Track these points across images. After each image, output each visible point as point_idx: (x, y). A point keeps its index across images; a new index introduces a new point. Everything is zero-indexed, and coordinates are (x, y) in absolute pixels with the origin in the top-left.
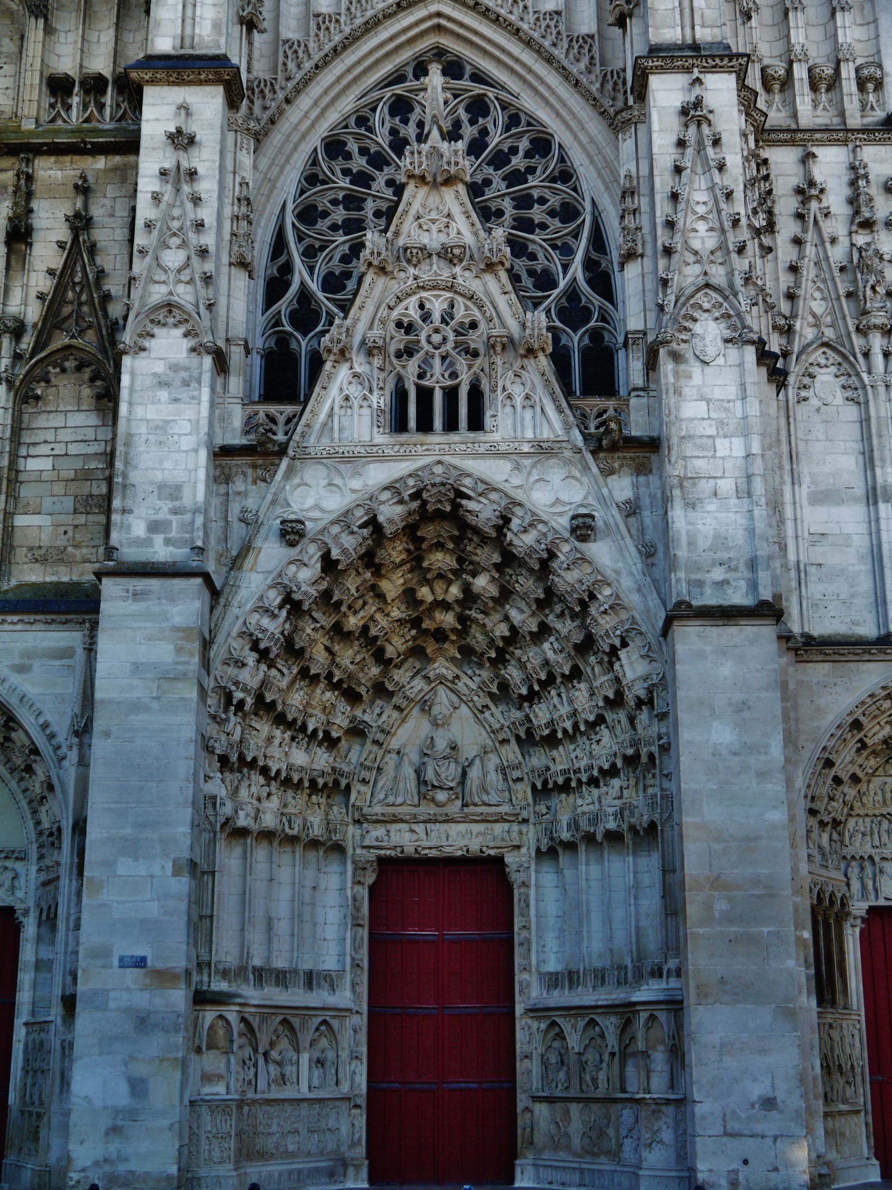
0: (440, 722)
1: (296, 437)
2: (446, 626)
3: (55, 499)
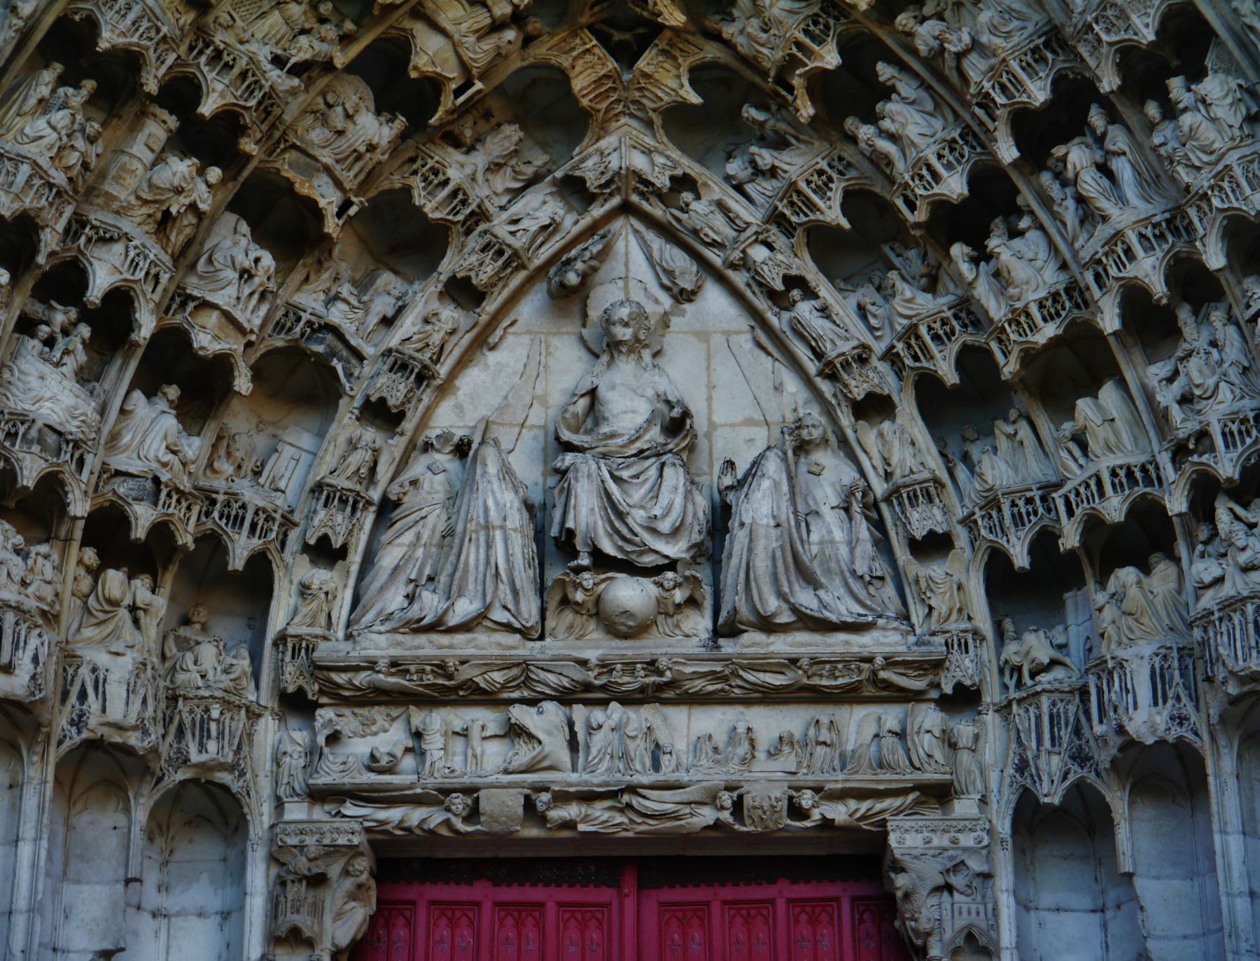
0: (624, 333)
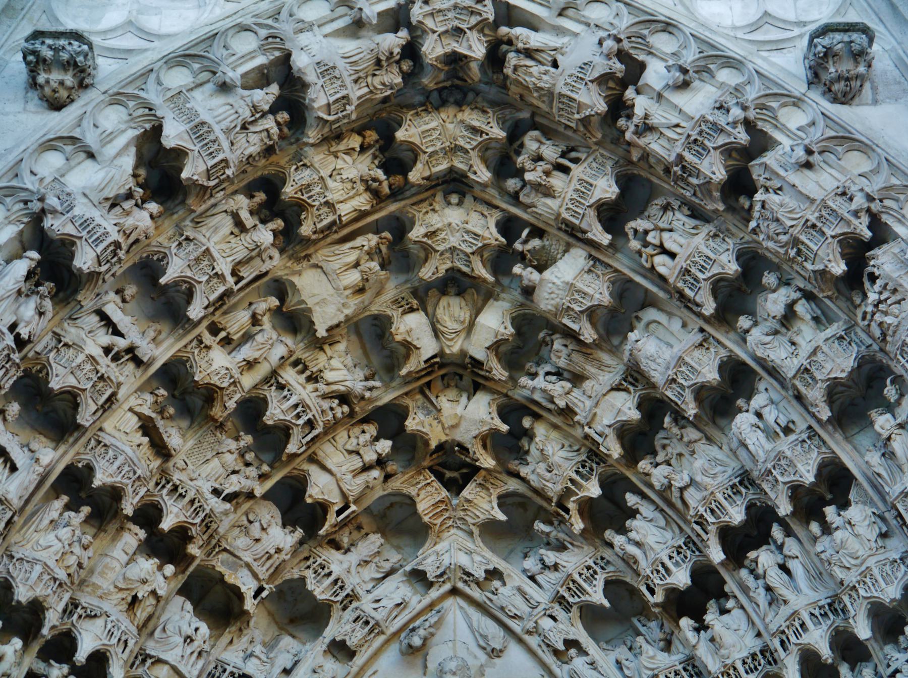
2: (466, 435)
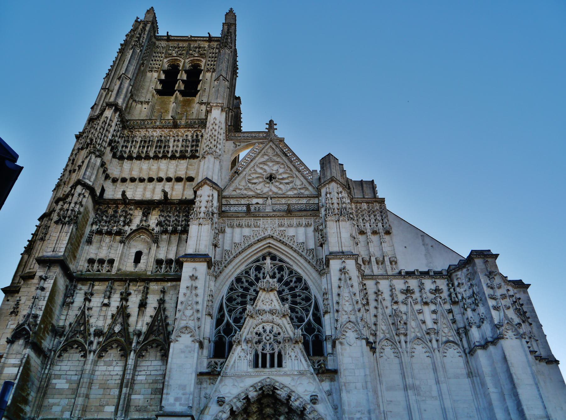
1: (223, 369)
3: (145, 389)
